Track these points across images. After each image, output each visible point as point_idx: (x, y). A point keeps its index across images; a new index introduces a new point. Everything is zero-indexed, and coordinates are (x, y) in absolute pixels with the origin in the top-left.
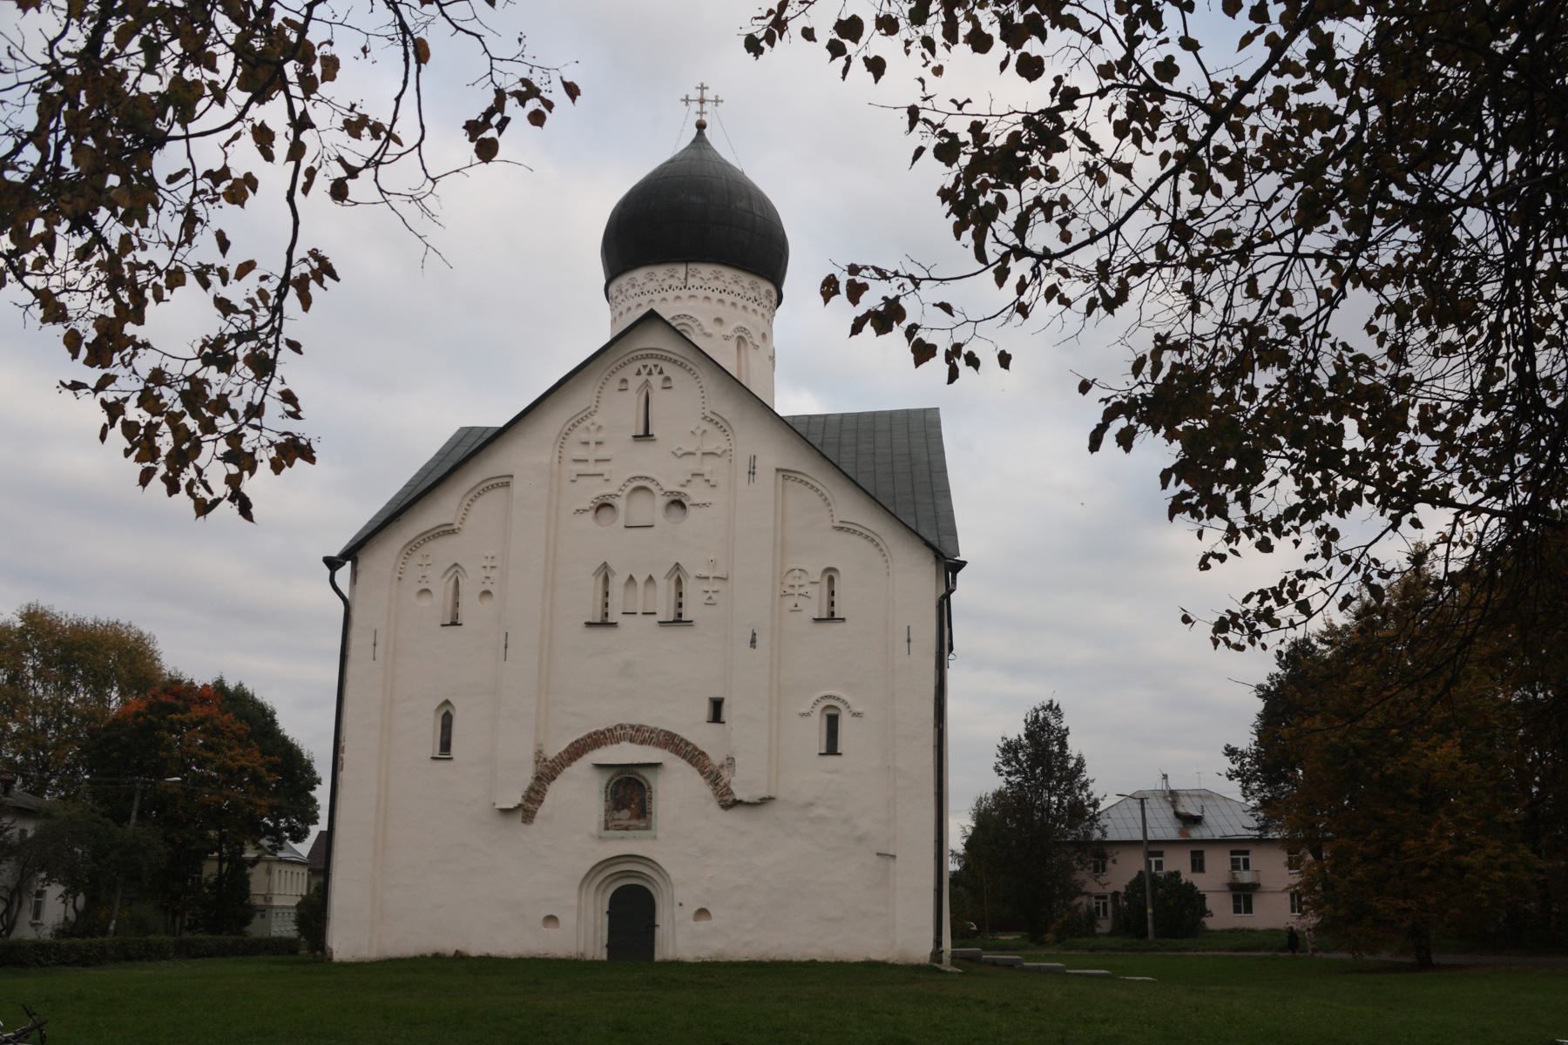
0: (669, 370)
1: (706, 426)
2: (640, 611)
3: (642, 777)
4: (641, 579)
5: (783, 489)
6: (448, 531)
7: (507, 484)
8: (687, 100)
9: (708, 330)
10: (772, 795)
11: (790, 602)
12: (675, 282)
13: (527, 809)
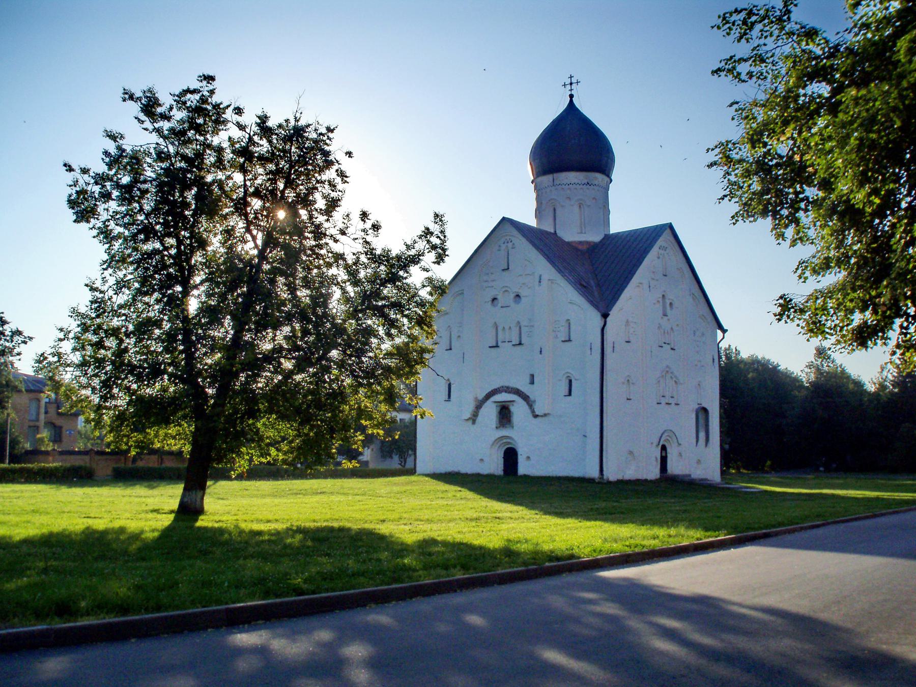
2: (507, 340)
4: (507, 328)
7: (463, 293)
13: (474, 418)
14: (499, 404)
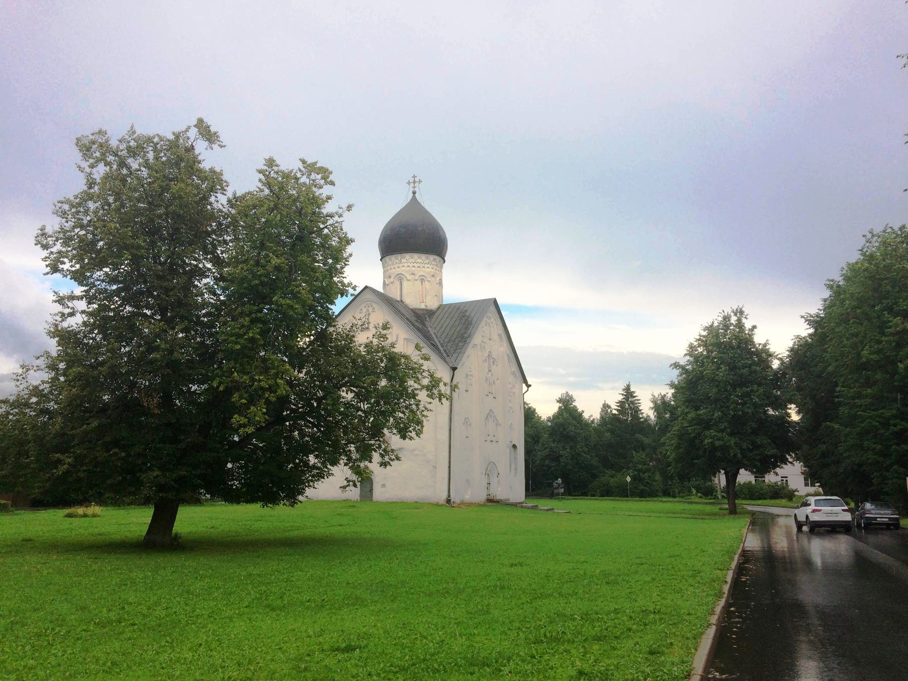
0: (374, 305)
8: (409, 183)
9: (409, 279)
10: (402, 446)
12: (397, 261)
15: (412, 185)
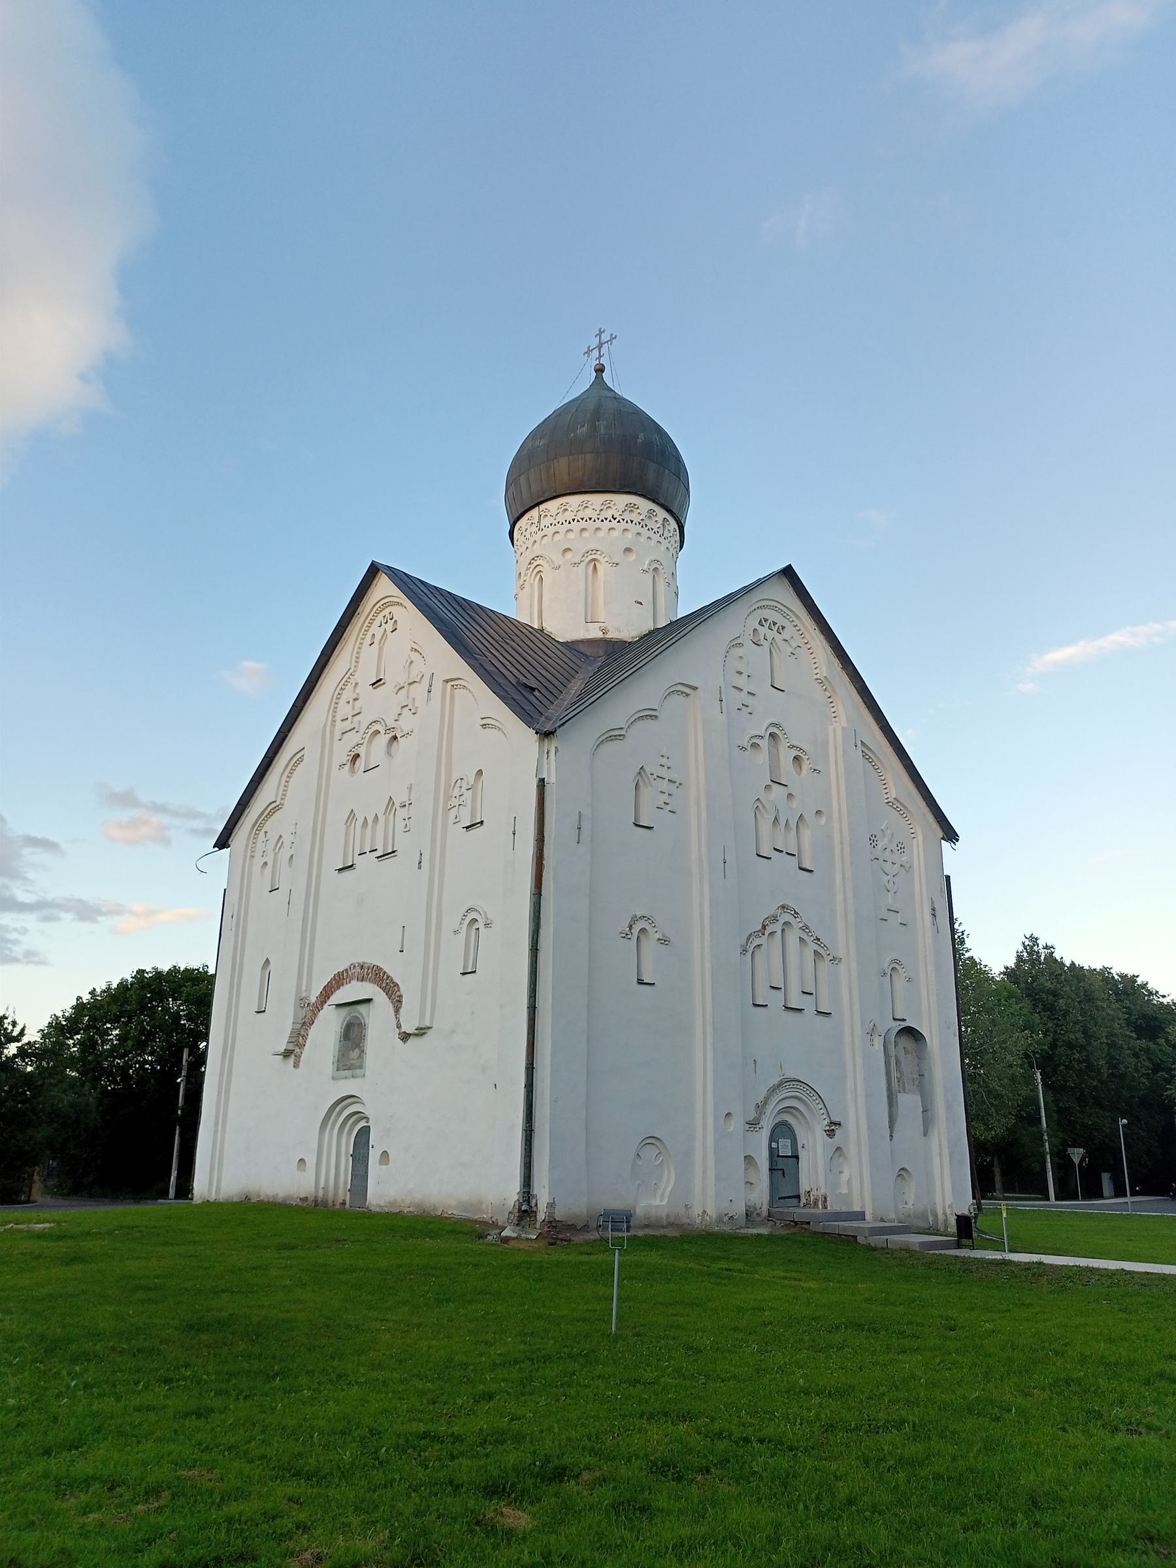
1: (415, 656)
2: (367, 850)
3: (361, 1014)
5: (452, 696)
6: (273, 809)
11: (453, 812)
12: (534, 528)
14: (345, 1010)
15: (595, 353)
